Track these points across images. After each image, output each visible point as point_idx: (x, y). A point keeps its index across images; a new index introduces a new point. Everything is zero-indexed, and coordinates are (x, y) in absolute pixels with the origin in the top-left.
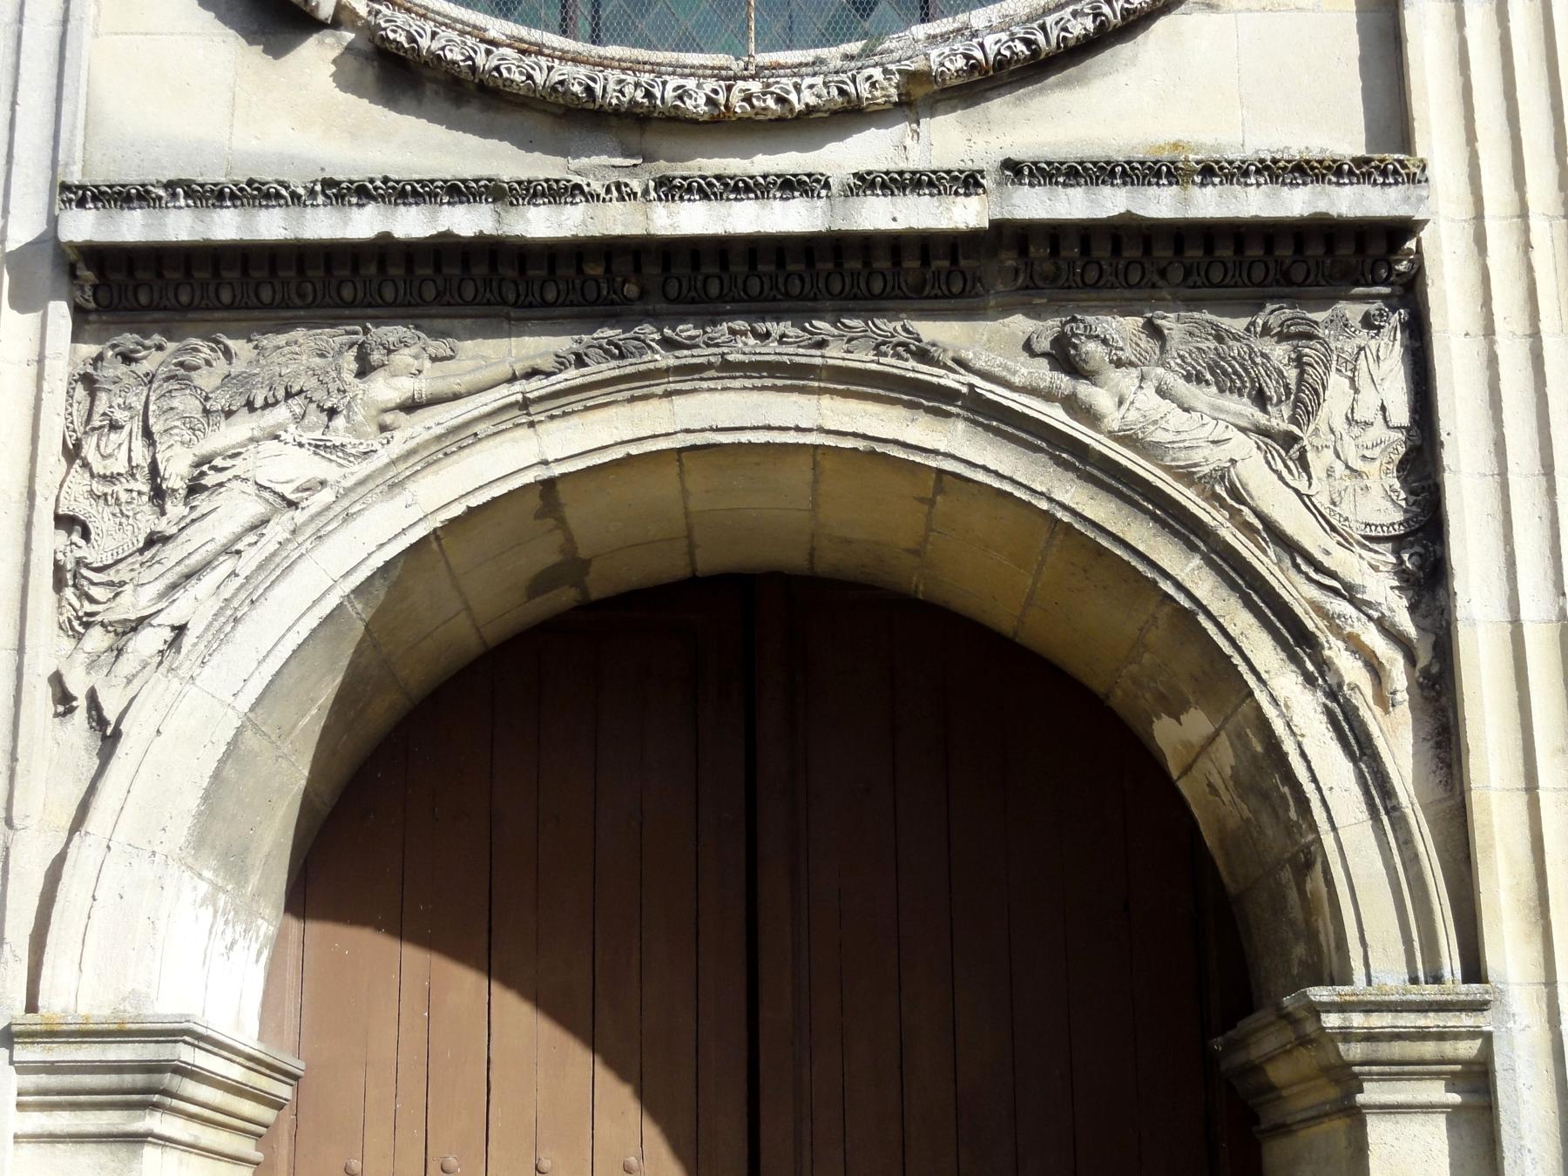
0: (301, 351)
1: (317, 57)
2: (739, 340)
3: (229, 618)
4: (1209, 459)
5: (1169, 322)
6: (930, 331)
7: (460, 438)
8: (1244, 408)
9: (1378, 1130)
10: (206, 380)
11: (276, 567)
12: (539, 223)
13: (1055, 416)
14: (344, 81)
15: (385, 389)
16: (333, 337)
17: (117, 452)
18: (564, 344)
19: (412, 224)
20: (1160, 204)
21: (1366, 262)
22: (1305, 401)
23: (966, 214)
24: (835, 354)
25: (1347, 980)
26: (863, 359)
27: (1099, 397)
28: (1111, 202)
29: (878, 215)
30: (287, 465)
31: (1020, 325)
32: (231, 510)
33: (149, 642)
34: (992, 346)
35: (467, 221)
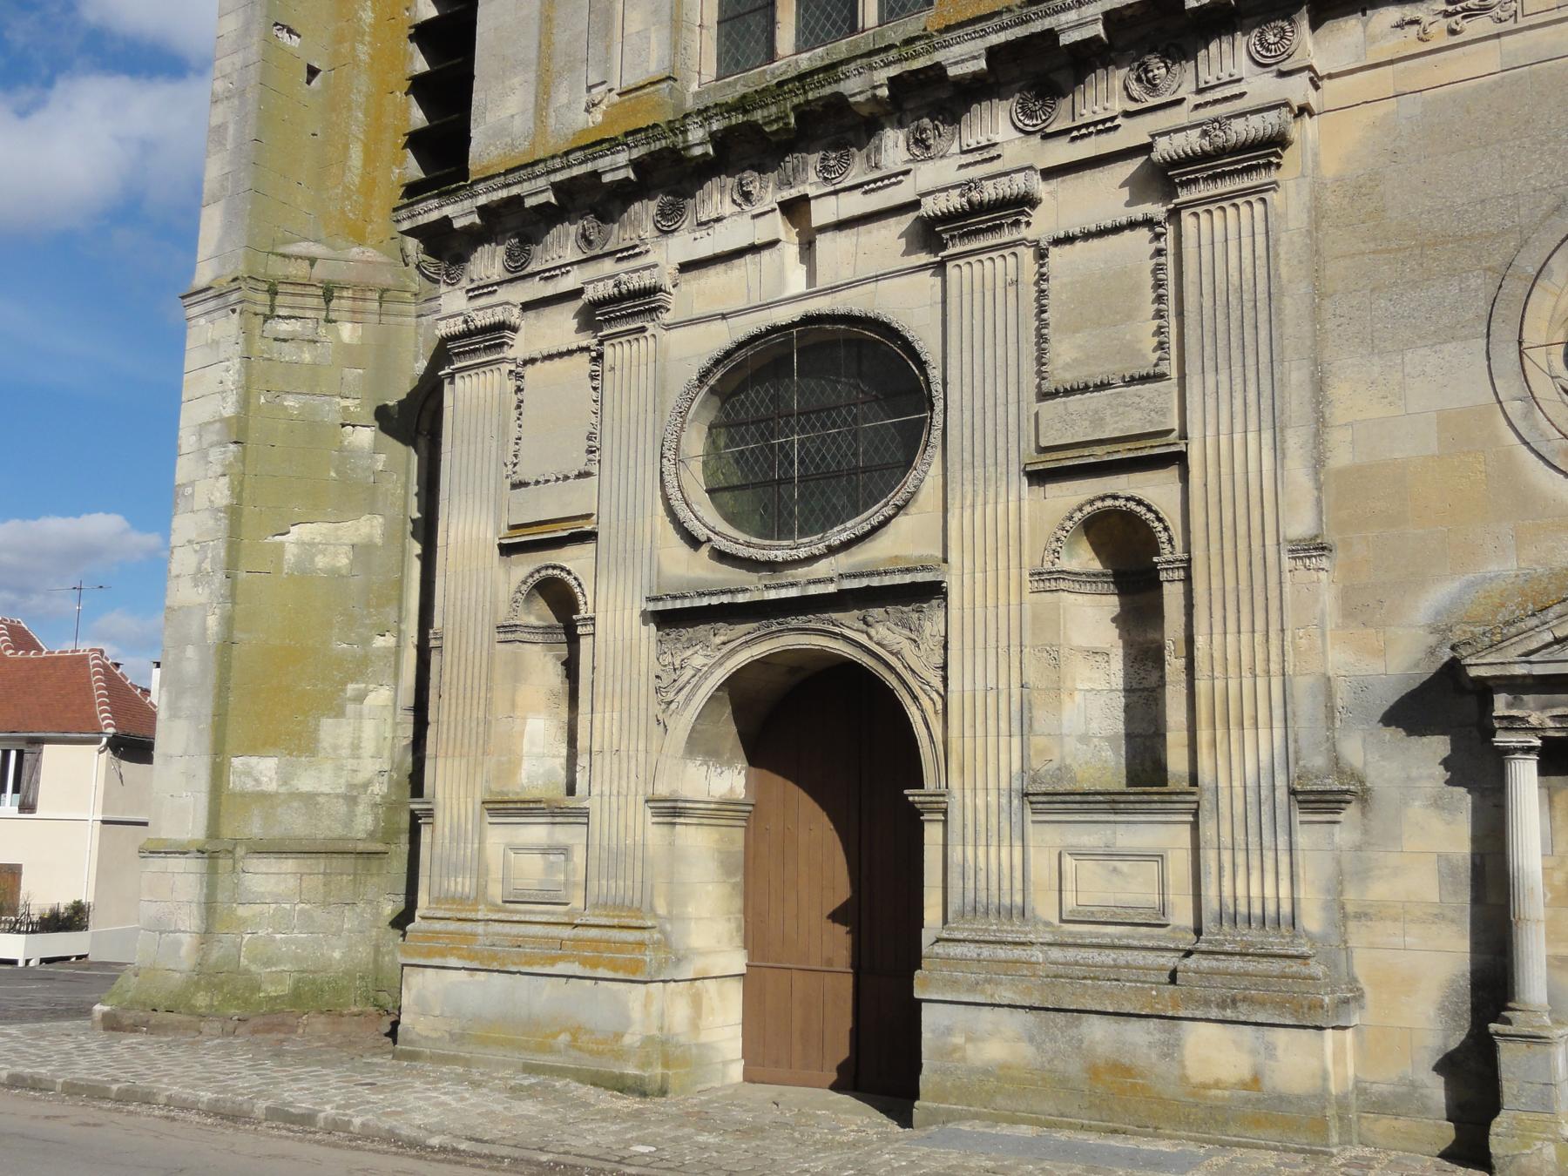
0: (702, 630)
1: (705, 550)
2: (794, 622)
3: (688, 700)
4: (896, 648)
5: (889, 609)
6: (834, 616)
7: (733, 652)
8: (907, 632)
9: (927, 826)
10: (684, 639)
11: (697, 687)
12: (741, 598)
13: (862, 639)
14: (711, 557)
15: (719, 640)
16: (708, 627)
17: (668, 659)
18: (755, 625)
19: (715, 601)
20: (875, 582)
21: (933, 591)
22: (920, 629)
23: (832, 588)
24: (812, 625)
25: (922, 787)
26: (819, 626)
27: (872, 632)
28: (864, 582)
29: (813, 590)
30: (698, 661)
31: (856, 612)
32: (688, 673)
33: (673, 706)
34: (848, 621)
35: (726, 599)
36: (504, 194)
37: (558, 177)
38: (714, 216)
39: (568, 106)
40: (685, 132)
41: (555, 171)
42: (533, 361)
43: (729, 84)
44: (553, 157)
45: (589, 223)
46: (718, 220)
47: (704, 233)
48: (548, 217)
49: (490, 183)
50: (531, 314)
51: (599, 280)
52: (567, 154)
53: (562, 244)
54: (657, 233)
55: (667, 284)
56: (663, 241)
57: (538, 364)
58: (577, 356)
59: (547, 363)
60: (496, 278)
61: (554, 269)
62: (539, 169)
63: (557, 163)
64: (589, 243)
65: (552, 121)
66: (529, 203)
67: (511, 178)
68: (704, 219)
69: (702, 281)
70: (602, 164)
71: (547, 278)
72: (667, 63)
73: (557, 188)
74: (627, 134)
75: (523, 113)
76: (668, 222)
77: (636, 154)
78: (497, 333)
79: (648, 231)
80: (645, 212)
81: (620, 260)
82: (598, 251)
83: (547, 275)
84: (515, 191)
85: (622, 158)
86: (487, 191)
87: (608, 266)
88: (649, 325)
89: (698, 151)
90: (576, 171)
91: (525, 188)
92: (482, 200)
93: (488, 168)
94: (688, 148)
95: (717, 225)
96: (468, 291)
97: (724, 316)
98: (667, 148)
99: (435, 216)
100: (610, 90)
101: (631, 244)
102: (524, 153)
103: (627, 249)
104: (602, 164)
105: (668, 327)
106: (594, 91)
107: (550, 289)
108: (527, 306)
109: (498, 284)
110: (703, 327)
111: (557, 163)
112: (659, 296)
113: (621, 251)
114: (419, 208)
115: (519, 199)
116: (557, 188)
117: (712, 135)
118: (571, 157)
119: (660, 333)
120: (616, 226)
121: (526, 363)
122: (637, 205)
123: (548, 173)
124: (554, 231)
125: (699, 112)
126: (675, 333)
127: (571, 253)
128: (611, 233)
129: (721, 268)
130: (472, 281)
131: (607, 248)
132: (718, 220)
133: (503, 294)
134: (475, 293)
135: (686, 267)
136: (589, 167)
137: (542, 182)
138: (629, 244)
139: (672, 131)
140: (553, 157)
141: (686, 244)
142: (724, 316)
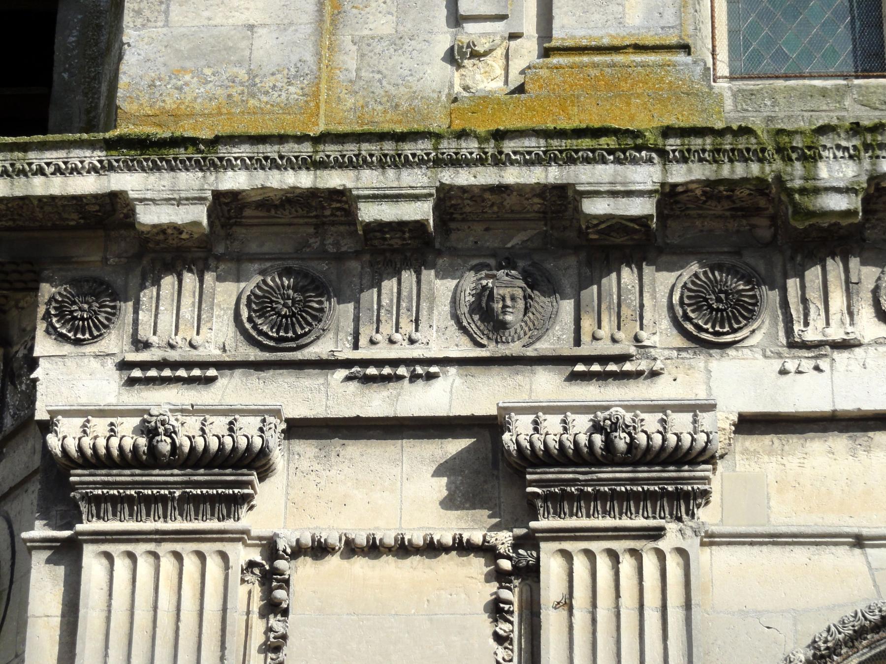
36: (305, 180)
37: (463, 178)
38: (836, 333)
39: (397, 41)
40: (810, 157)
41: (456, 162)
42: (319, 550)
43: (824, 93)
44: (462, 134)
45: (507, 286)
46: (844, 345)
47: (807, 365)
48: (401, 249)
49: (272, 151)
50: (306, 449)
51: (543, 407)
52: (499, 136)
53: (426, 312)
54: (679, 341)
55: (719, 445)
56: (700, 361)
57: (333, 561)
58: (449, 563)
59: (360, 564)
60: (212, 352)
61: (395, 363)
62: (423, 147)
63: (470, 147)
64: (497, 326)
65: (349, 60)
66: (369, 213)
67: (332, 150)
68: (811, 335)
69: (792, 462)
70: (584, 175)
71: (367, 380)
72: (670, 18)
73: (447, 200)
74: (667, 132)
75: (283, 27)
76: (711, 321)
77: (679, 174)
78: (226, 474)
79: (660, 335)
80: (655, 291)
81: (574, 377)
82: (514, 349)
83: (370, 373)
84: (334, 179)
85: (646, 175)
86: (247, 165)
87: (546, 385)
88: (672, 527)
89: (838, 203)
90: (512, 176)
91: (368, 180)
92: (235, 180)
93: (175, 116)
94: (817, 191)
95: (841, 357)
96: (124, 366)
97: (859, 541)
98: (760, 181)
99: (86, 185)
100: (513, 36)
101: (616, 350)
102: (287, 108)
103: (603, 360)
104: (584, 175)
105: (711, 540)
106: (471, 28)
107: (377, 403)
108: (298, 429)
109: (220, 365)
110: (800, 554)
111: (470, 147)
112: (703, 470)
113: (588, 360)
114: (36, 158)
115: (342, 199)
116: (447, 200)
117: (875, 179)
118: (509, 146)
119: (691, 544)
120: (567, 306)
121: (298, 551)
122: (628, 276)
123: (439, 163)
124: (389, 286)
125: (856, 129)
126: (723, 555)
127: (440, 339)
128: (553, 317)
129: (839, 442)
130: (141, 344)
131: (544, 347)
132: (844, 345)
133: (230, 390)
134: (136, 373)
135: (750, 424)
136: (553, 175)
137: (416, 179)
138: (605, 348)
139: (779, 150)
140: (462, 134)
141: (746, 376)
142: (859, 541)
